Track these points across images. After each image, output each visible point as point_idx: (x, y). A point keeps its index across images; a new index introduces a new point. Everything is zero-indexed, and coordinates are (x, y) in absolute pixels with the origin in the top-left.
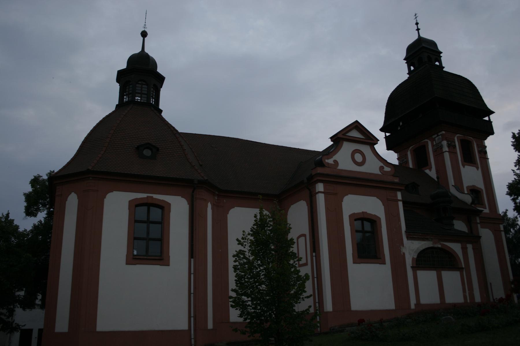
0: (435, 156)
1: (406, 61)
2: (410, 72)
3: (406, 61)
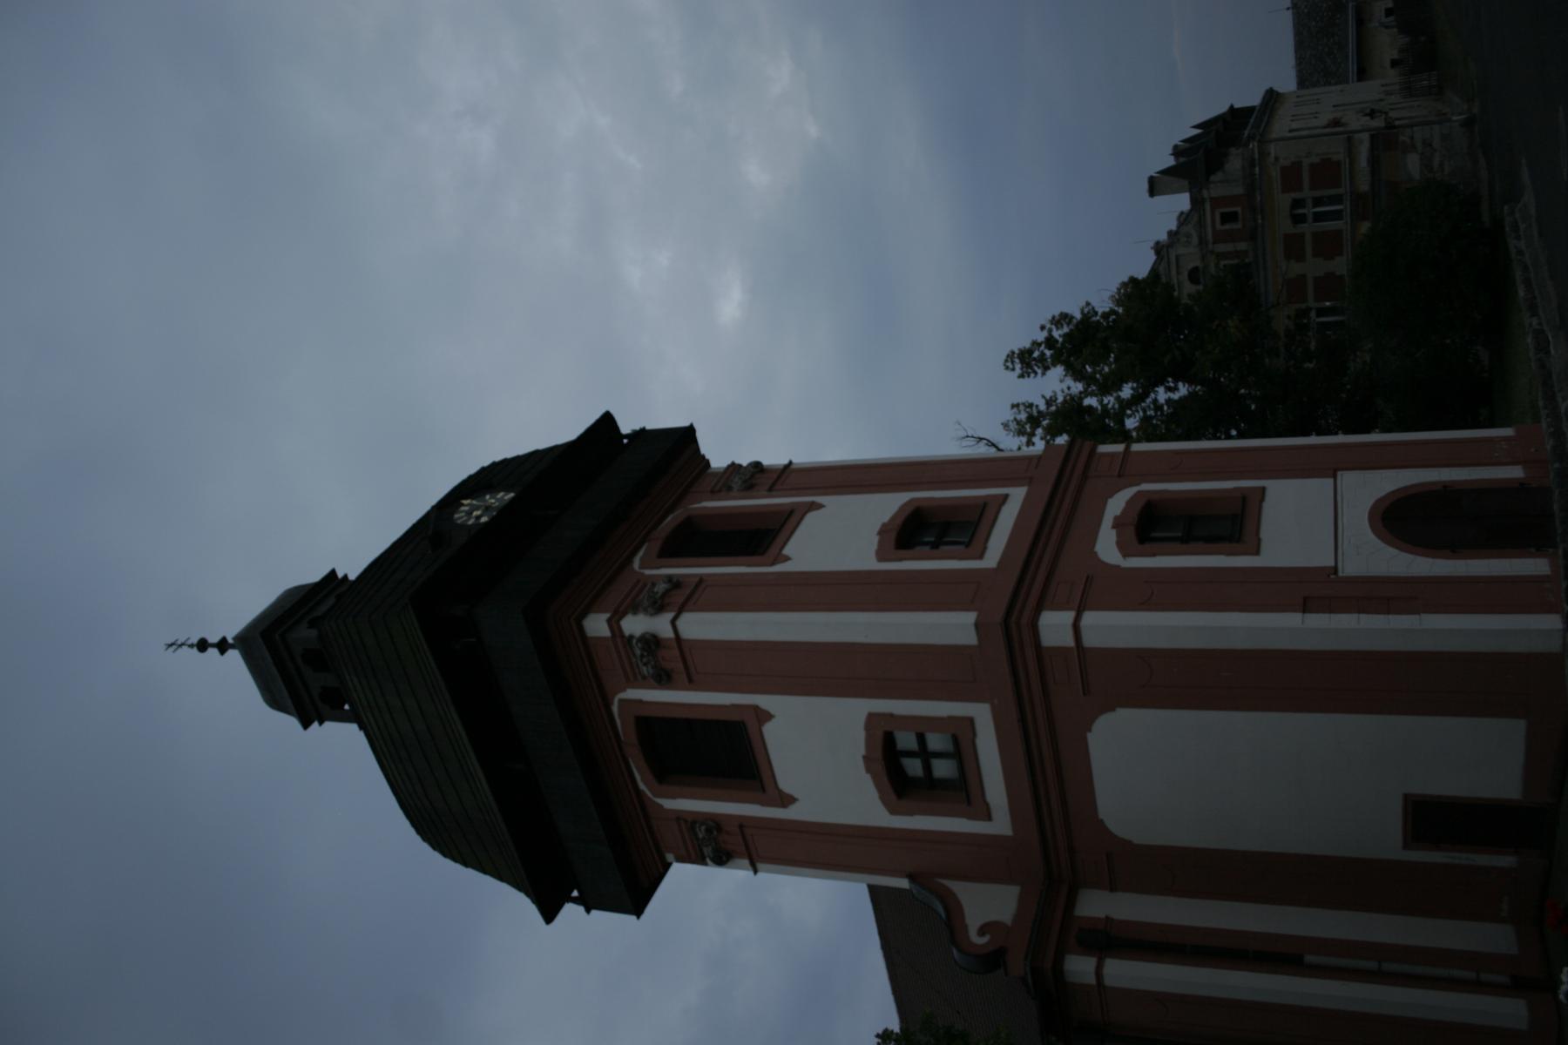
0: (692, 683)
1: (316, 724)
3: (316, 724)
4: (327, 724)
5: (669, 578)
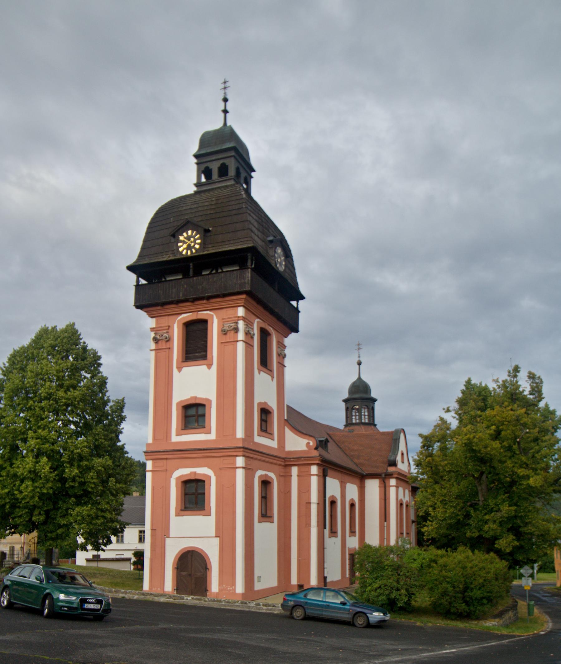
0: (221, 343)
2: (198, 184)
4: (195, 167)
5: (254, 335)
